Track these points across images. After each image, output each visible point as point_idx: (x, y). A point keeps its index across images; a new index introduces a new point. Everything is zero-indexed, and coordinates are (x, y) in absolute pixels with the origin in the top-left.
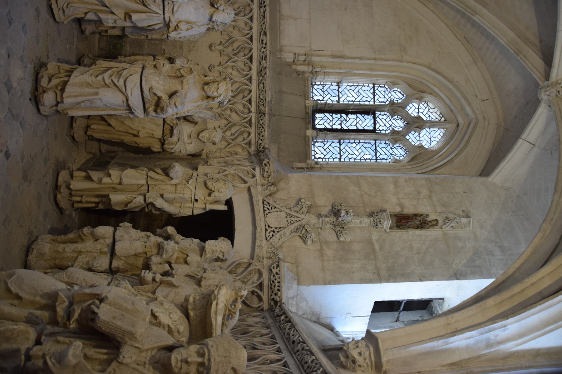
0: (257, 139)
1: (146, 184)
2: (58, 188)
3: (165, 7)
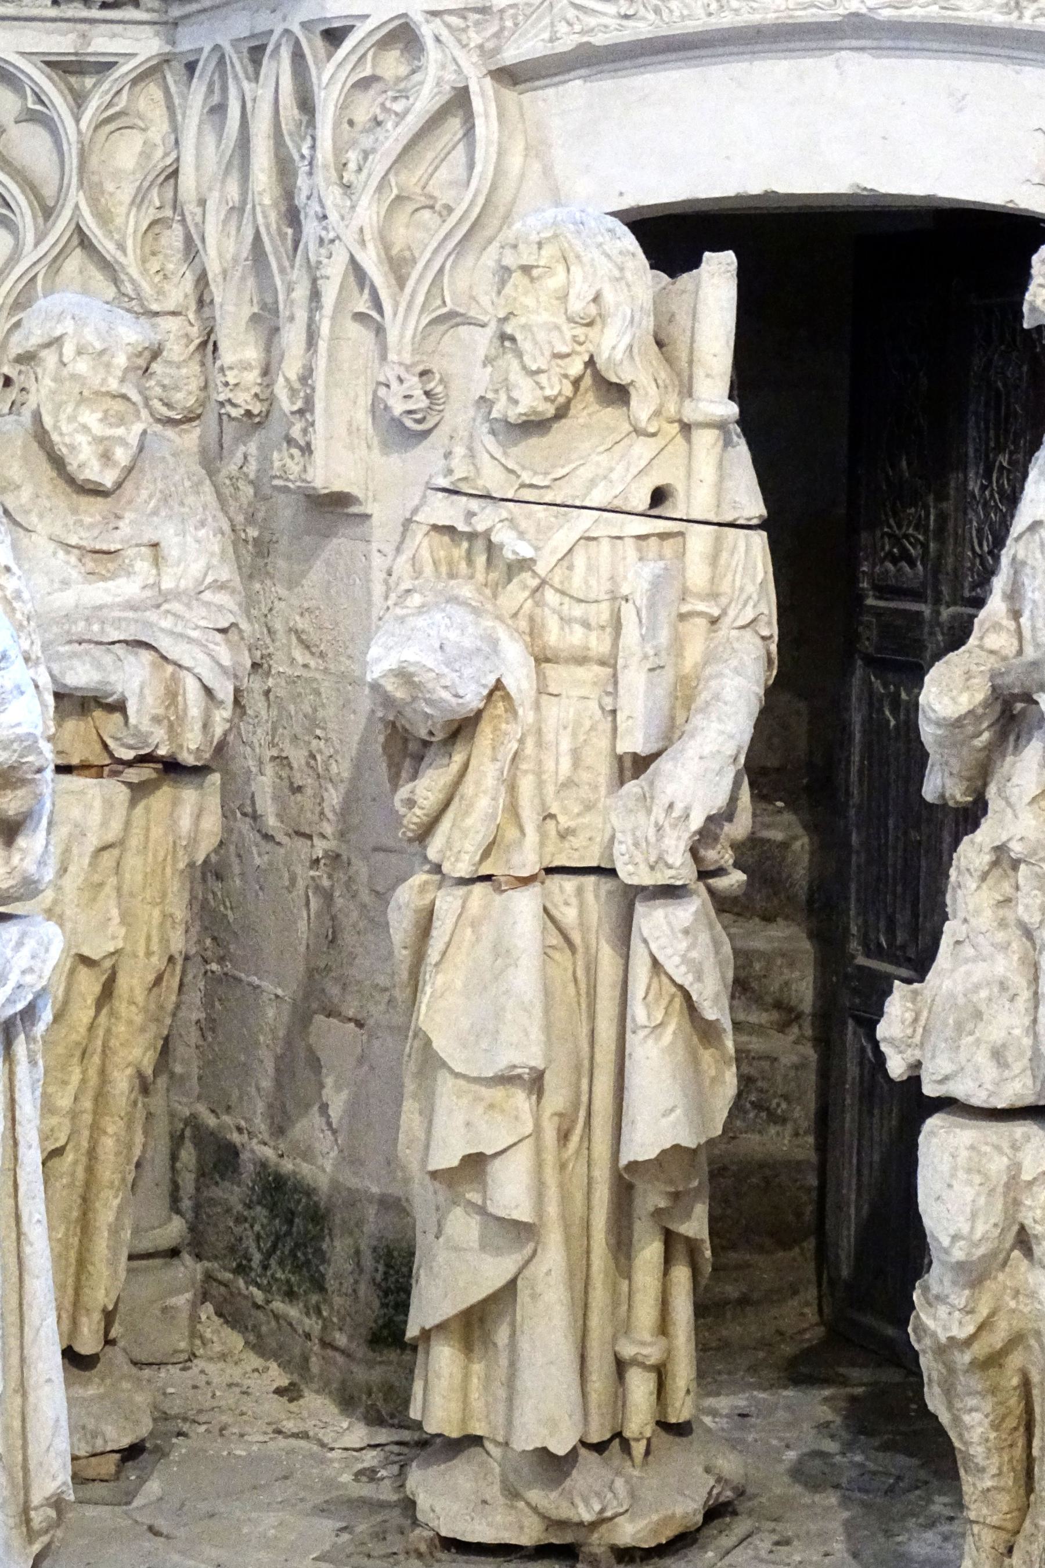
1: (535, 889)
2: (568, 1538)
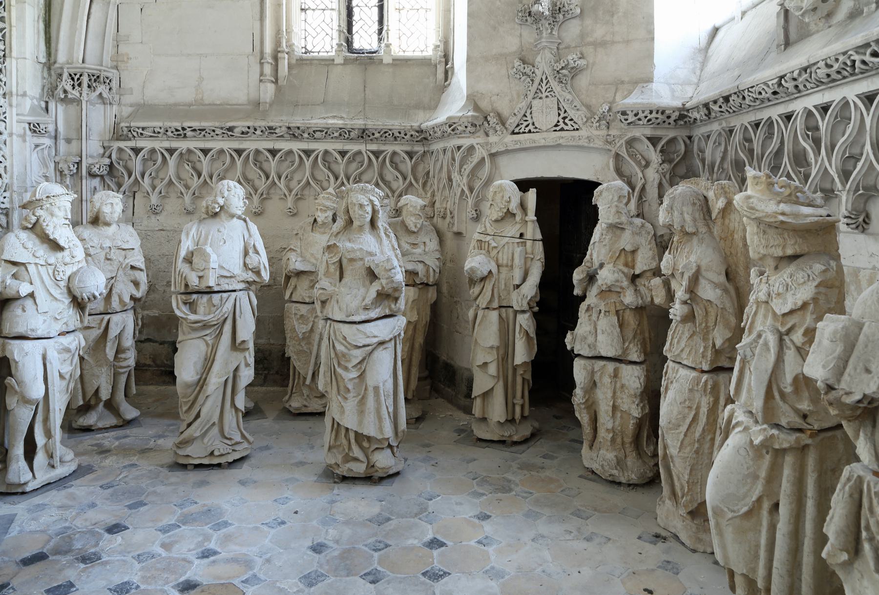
0: (403, 141)
3: (223, 289)
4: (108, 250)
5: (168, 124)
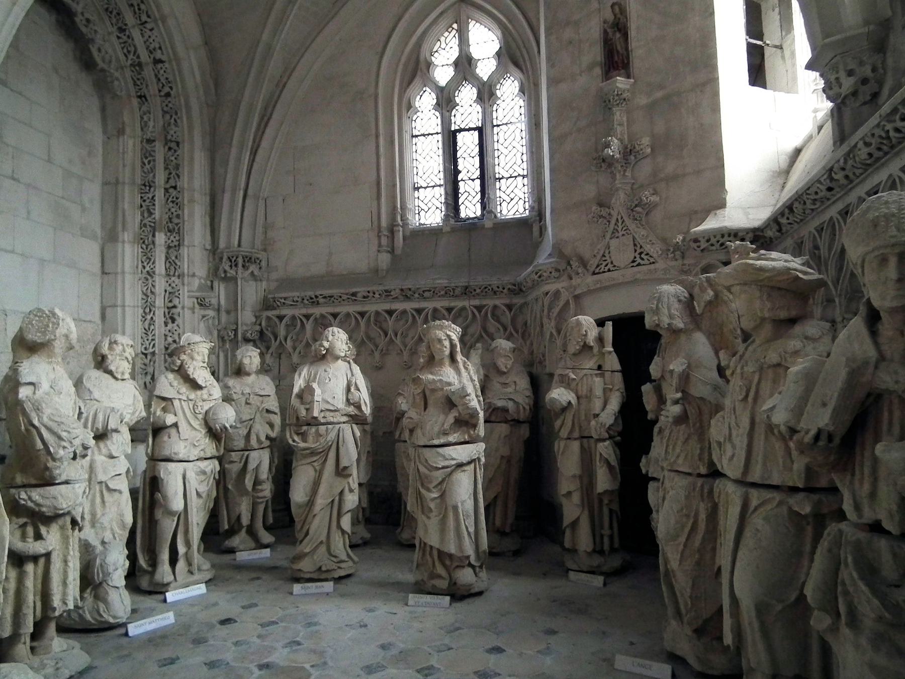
4: (248, 396)
5: (303, 294)
